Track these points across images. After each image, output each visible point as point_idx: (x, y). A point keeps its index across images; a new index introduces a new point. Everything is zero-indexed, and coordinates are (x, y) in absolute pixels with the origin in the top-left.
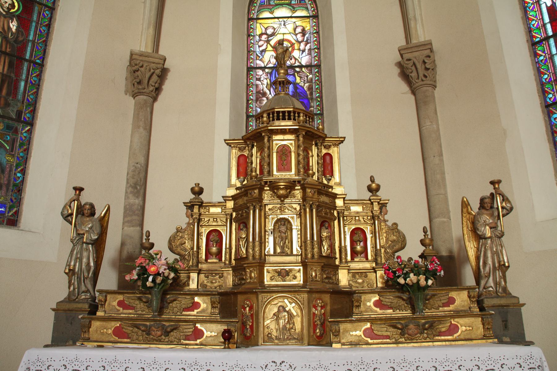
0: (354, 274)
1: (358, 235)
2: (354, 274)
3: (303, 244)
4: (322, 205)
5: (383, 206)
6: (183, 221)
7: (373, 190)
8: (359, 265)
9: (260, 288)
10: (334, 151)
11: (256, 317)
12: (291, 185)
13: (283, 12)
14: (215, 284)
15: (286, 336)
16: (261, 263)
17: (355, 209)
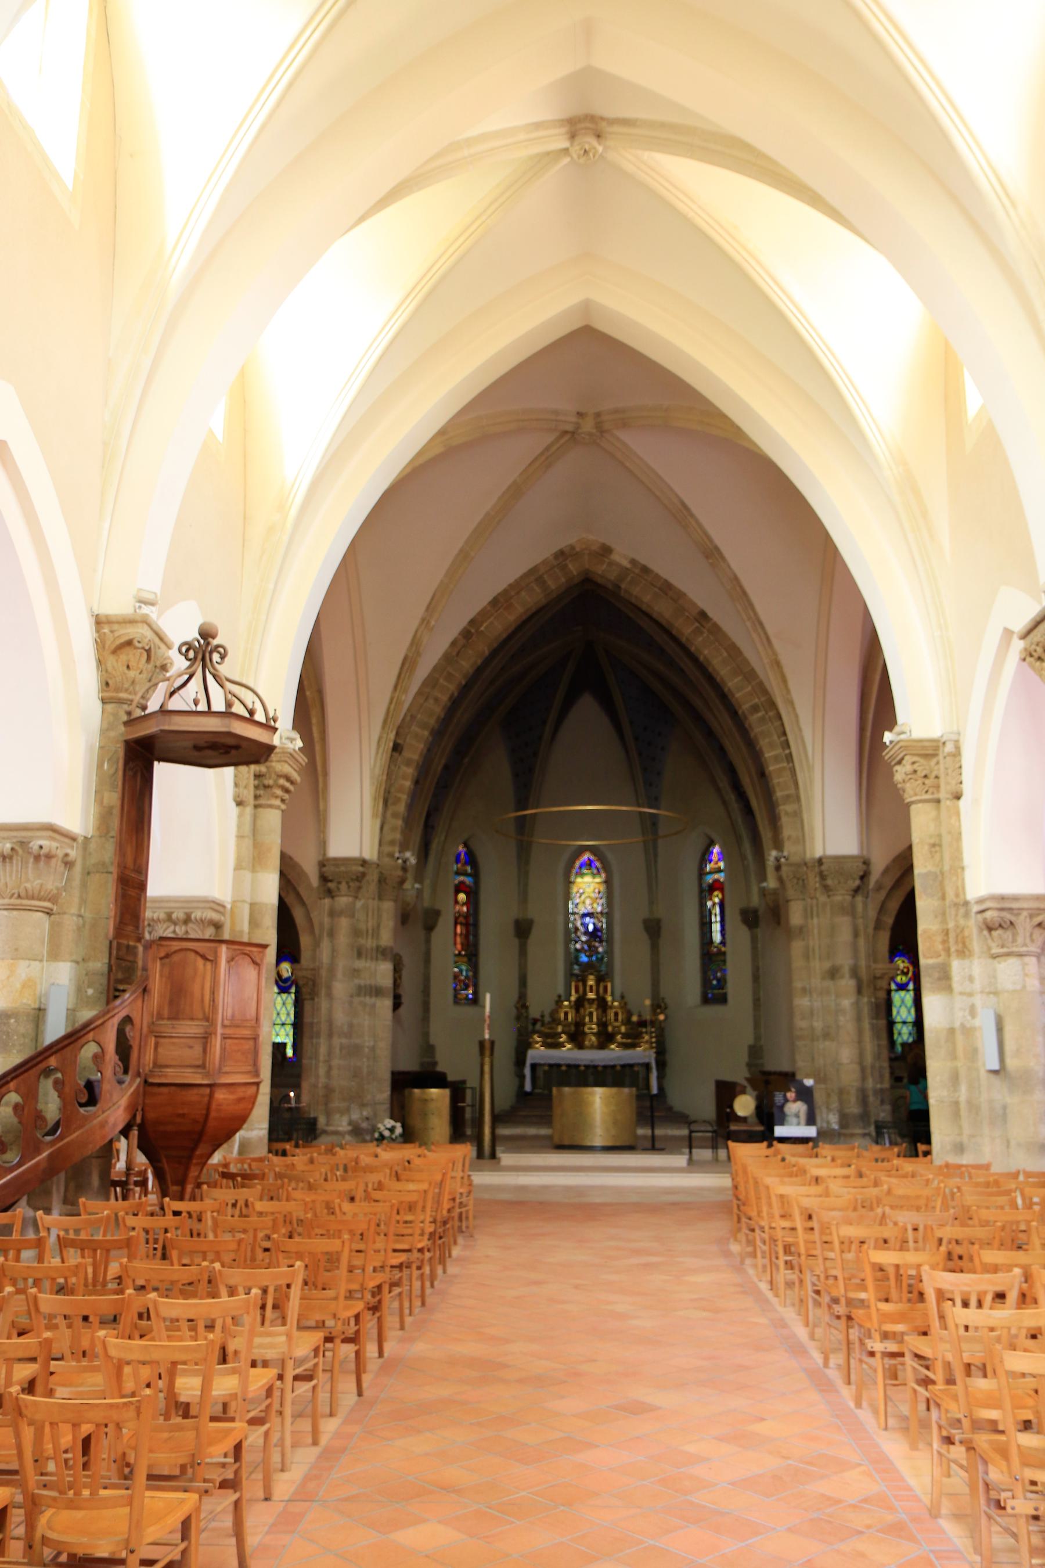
0: (614, 1027)
1: (616, 1014)
2: (614, 1027)
3: (598, 1018)
4: (602, 1004)
5: (626, 1004)
6: (553, 1006)
7: (622, 997)
8: (617, 1024)
9: (584, 1034)
10: (609, 985)
11: (583, 1041)
12: (593, 1000)
13: (588, 879)
14: (567, 1029)
15: (592, 1047)
16: (584, 1025)
17: (616, 1004)
